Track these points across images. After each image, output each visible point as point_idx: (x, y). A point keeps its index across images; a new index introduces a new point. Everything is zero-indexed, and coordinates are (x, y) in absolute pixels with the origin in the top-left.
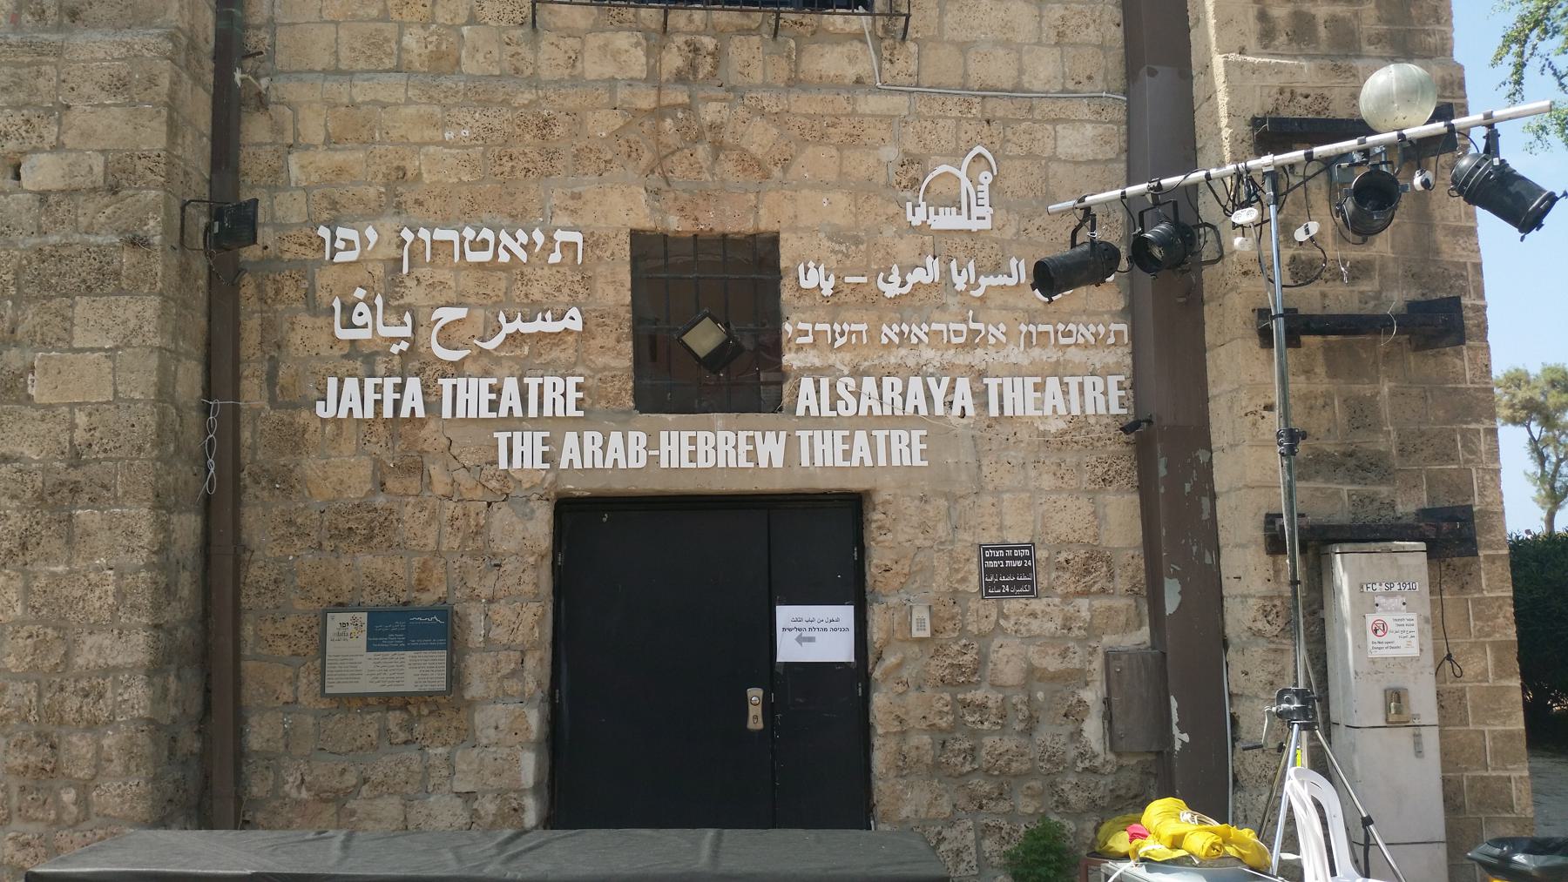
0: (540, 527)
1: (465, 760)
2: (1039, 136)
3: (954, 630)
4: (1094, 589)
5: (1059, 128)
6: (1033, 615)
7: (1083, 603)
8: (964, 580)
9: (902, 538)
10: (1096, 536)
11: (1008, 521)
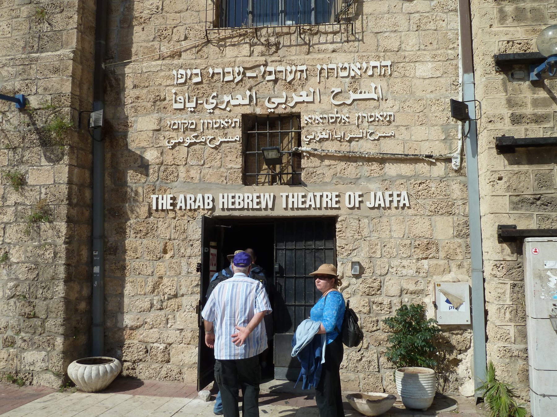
2: (408, 68)
3: (370, 273)
4: (430, 256)
5: (417, 64)
6: (404, 267)
7: (425, 262)
8: (374, 252)
9: (349, 235)
10: (431, 234)
11: (394, 228)
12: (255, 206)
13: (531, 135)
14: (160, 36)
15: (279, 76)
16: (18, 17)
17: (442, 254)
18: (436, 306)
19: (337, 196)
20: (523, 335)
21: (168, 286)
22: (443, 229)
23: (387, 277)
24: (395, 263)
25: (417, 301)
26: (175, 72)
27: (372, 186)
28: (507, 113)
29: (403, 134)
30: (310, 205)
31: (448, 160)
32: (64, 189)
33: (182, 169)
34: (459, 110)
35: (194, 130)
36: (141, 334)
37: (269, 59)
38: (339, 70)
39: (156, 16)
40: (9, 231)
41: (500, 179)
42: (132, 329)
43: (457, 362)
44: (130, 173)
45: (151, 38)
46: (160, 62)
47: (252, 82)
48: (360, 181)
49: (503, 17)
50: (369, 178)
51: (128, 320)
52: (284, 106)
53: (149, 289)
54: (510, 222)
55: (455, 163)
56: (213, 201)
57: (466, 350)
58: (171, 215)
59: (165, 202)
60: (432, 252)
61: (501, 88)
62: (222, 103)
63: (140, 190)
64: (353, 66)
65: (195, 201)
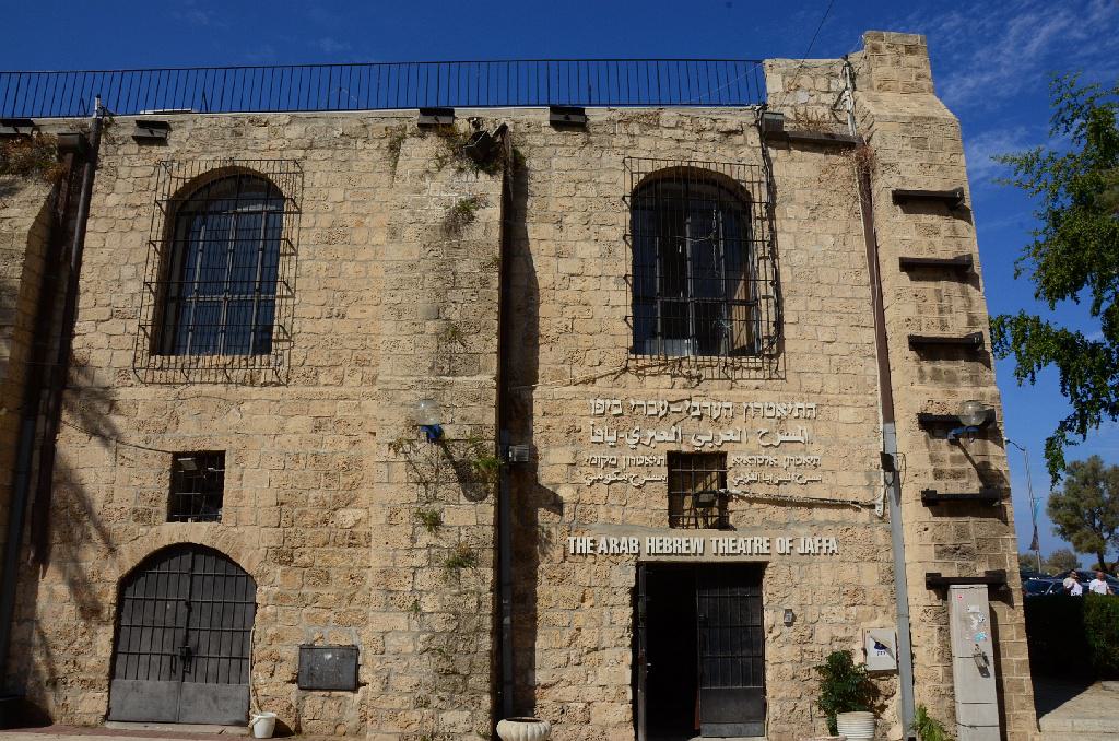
7: (854, 608)
12: (684, 551)
14: (571, 360)
15: (705, 412)
16: (422, 333)
17: (869, 601)
18: (865, 653)
19: (768, 541)
20: (949, 674)
21: (588, 639)
22: (870, 575)
23: (817, 625)
25: (846, 647)
26: (592, 401)
27: (802, 531)
28: (930, 468)
29: (829, 479)
30: (741, 551)
31: (872, 507)
32: (489, 531)
33: (602, 509)
34: (887, 461)
35: (615, 466)
36: (553, 694)
37: (694, 393)
38: (766, 410)
39: (567, 336)
40: (419, 576)
41: (926, 529)
42: (545, 687)
43: (883, 708)
44: (541, 511)
45: (561, 360)
46: (572, 388)
47: (676, 417)
48: (788, 527)
49: (922, 377)
50: (797, 523)
51: (541, 677)
52: (711, 444)
53: (565, 642)
54: (935, 570)
55: (879, 510)
56: (639, 545)
57: (893, 695)
58: (590, 559)
59: (584, 544)
60: (859, 598)
61: (924, 444)
62: (645, 438)
63: (553, 530)
64: (779, 407)
65: (619, 545)
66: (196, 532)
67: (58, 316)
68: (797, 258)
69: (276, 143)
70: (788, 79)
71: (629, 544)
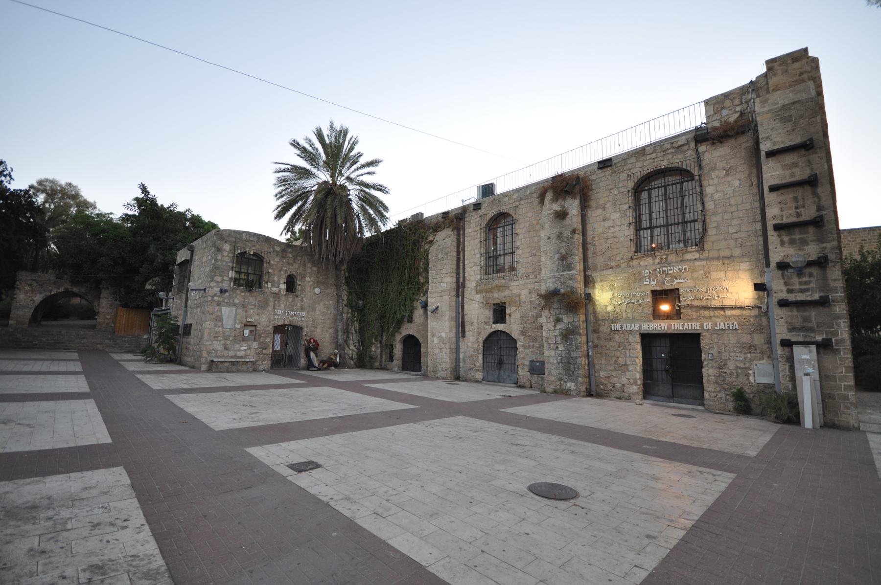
0: (638, 339)
1: (627, 373)
7: (749, 355)
13: (799, 299)
14: (611, 259)
24: (732, 354)
27: (718, 320)
28: (784, 289)
50: (718, 317)
54: (788, 337)
60: (753, 349)
66: (500, 327)
67: (461, 267)
68: (716, 197)
69: (511, 201)
70: (717, 106)
71: (635, 326)
